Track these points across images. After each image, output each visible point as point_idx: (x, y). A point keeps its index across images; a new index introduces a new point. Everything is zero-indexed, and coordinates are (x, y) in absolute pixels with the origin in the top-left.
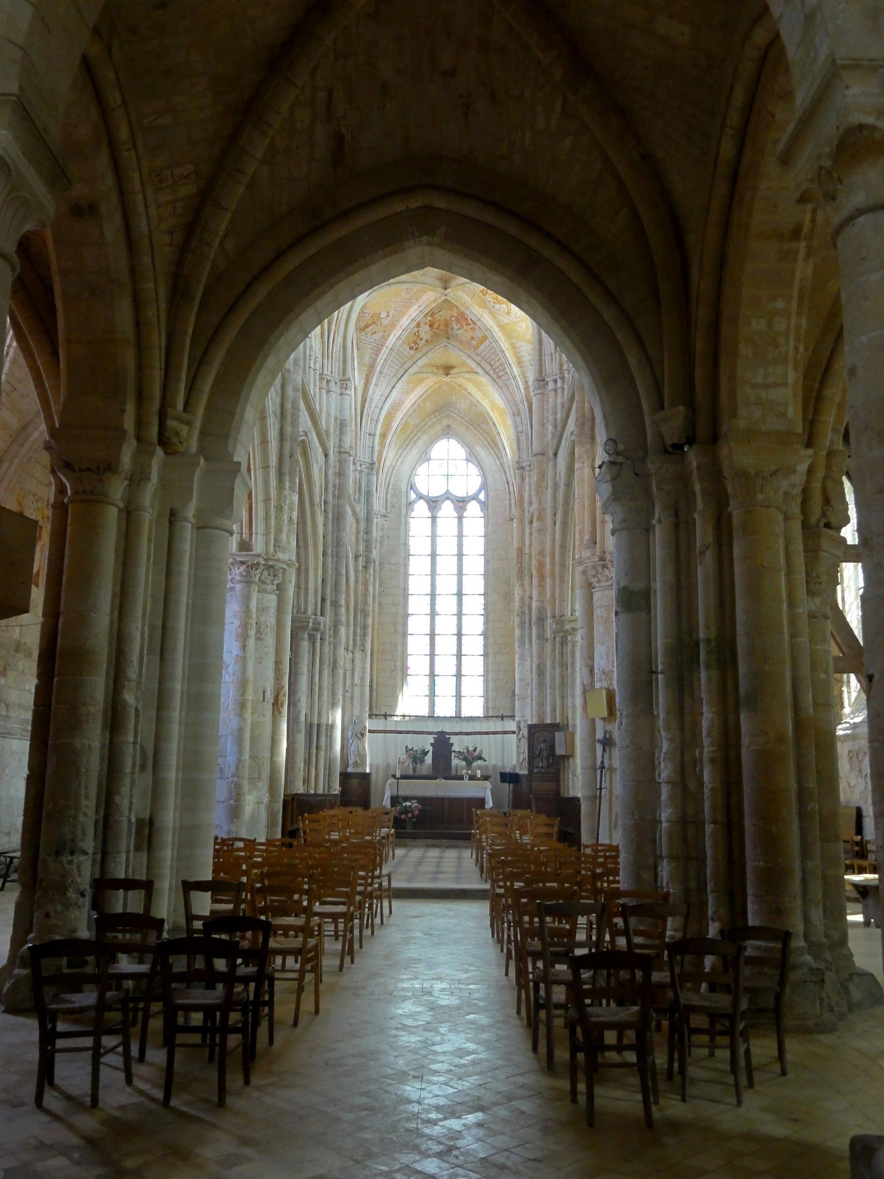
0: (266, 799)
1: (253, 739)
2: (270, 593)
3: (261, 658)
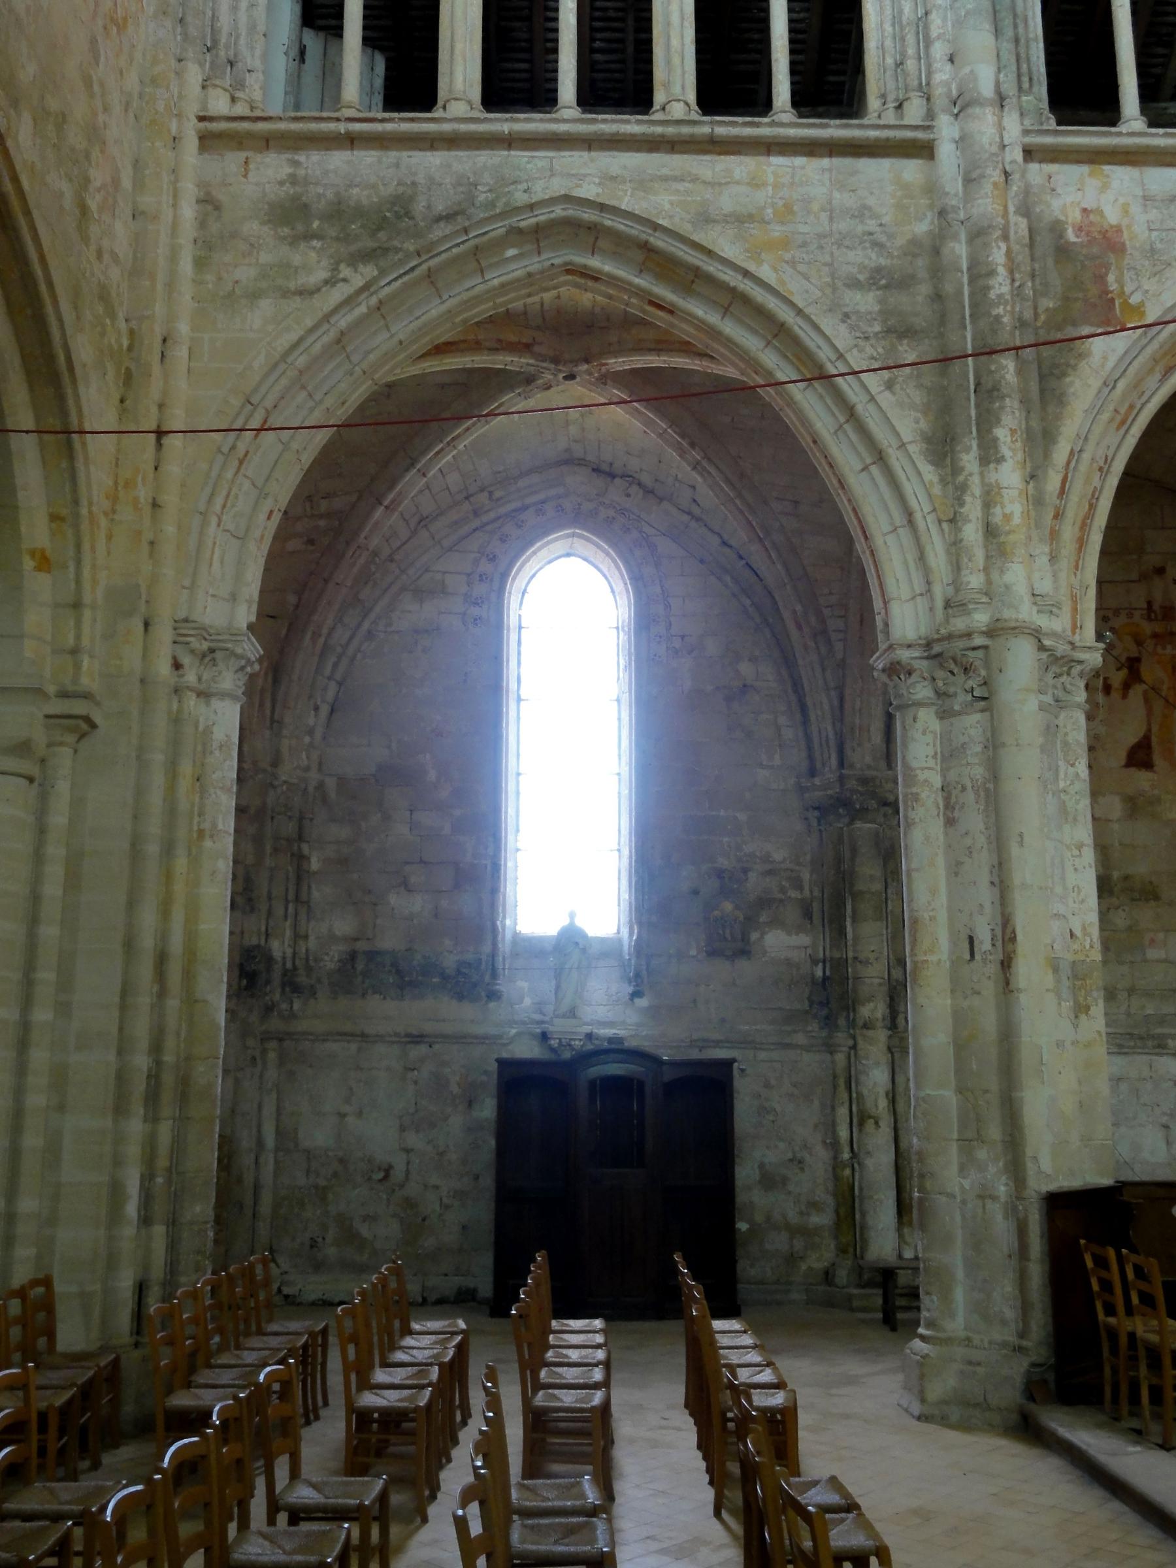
0: (1002, 1189)
1: (961, 1046)
2: (959, 713)
3: (959, 864)
